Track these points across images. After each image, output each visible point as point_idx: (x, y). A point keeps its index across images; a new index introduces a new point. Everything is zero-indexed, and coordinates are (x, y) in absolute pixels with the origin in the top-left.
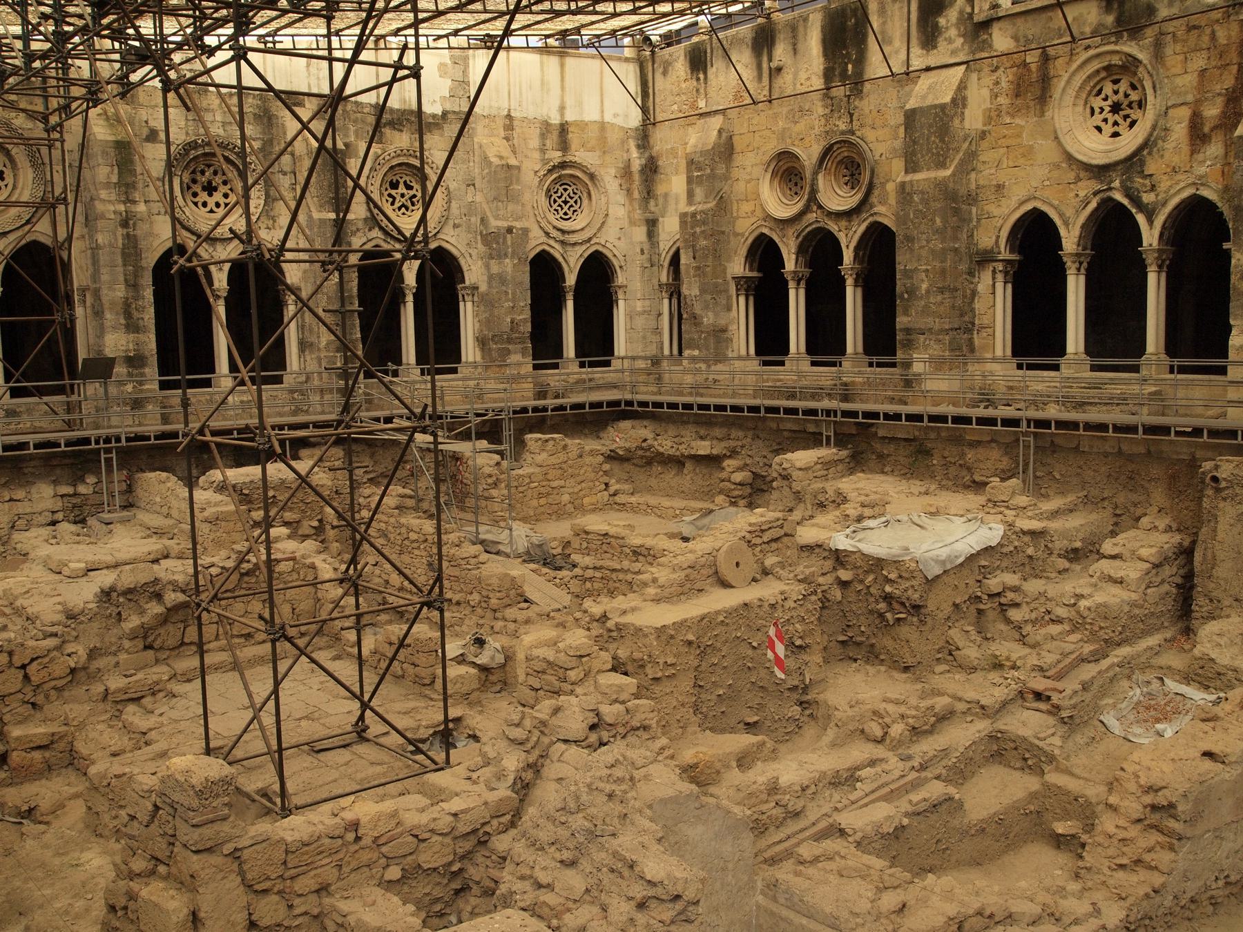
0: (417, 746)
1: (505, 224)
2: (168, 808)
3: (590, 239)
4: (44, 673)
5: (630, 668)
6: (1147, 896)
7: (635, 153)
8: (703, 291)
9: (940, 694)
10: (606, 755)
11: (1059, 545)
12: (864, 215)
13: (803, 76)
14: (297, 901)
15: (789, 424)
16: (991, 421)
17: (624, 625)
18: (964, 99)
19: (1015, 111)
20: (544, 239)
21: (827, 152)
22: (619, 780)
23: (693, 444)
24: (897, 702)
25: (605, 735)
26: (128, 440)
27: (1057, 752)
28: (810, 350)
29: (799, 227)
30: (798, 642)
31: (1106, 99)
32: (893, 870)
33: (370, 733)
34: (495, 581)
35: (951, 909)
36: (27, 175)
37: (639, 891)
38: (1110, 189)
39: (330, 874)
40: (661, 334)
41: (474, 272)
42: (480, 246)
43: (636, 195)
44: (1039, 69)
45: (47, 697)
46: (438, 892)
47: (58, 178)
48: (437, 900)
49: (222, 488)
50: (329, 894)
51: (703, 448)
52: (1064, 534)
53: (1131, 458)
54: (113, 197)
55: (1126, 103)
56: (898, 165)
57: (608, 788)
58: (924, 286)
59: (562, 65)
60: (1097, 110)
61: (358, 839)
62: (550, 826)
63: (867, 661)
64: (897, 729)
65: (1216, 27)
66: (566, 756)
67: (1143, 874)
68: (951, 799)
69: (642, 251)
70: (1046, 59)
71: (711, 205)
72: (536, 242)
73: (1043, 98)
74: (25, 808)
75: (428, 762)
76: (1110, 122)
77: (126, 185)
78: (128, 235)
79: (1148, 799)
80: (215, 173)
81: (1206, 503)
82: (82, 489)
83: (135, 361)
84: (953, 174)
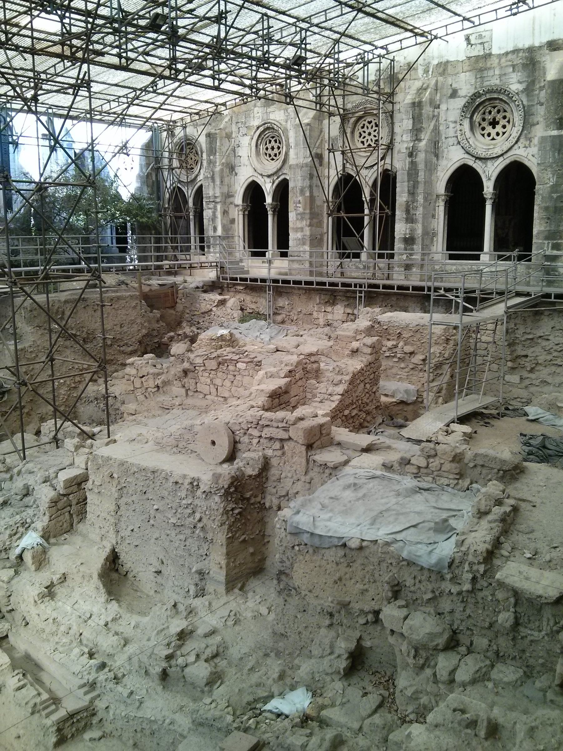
78: (412, 161)
80: (499, 111)
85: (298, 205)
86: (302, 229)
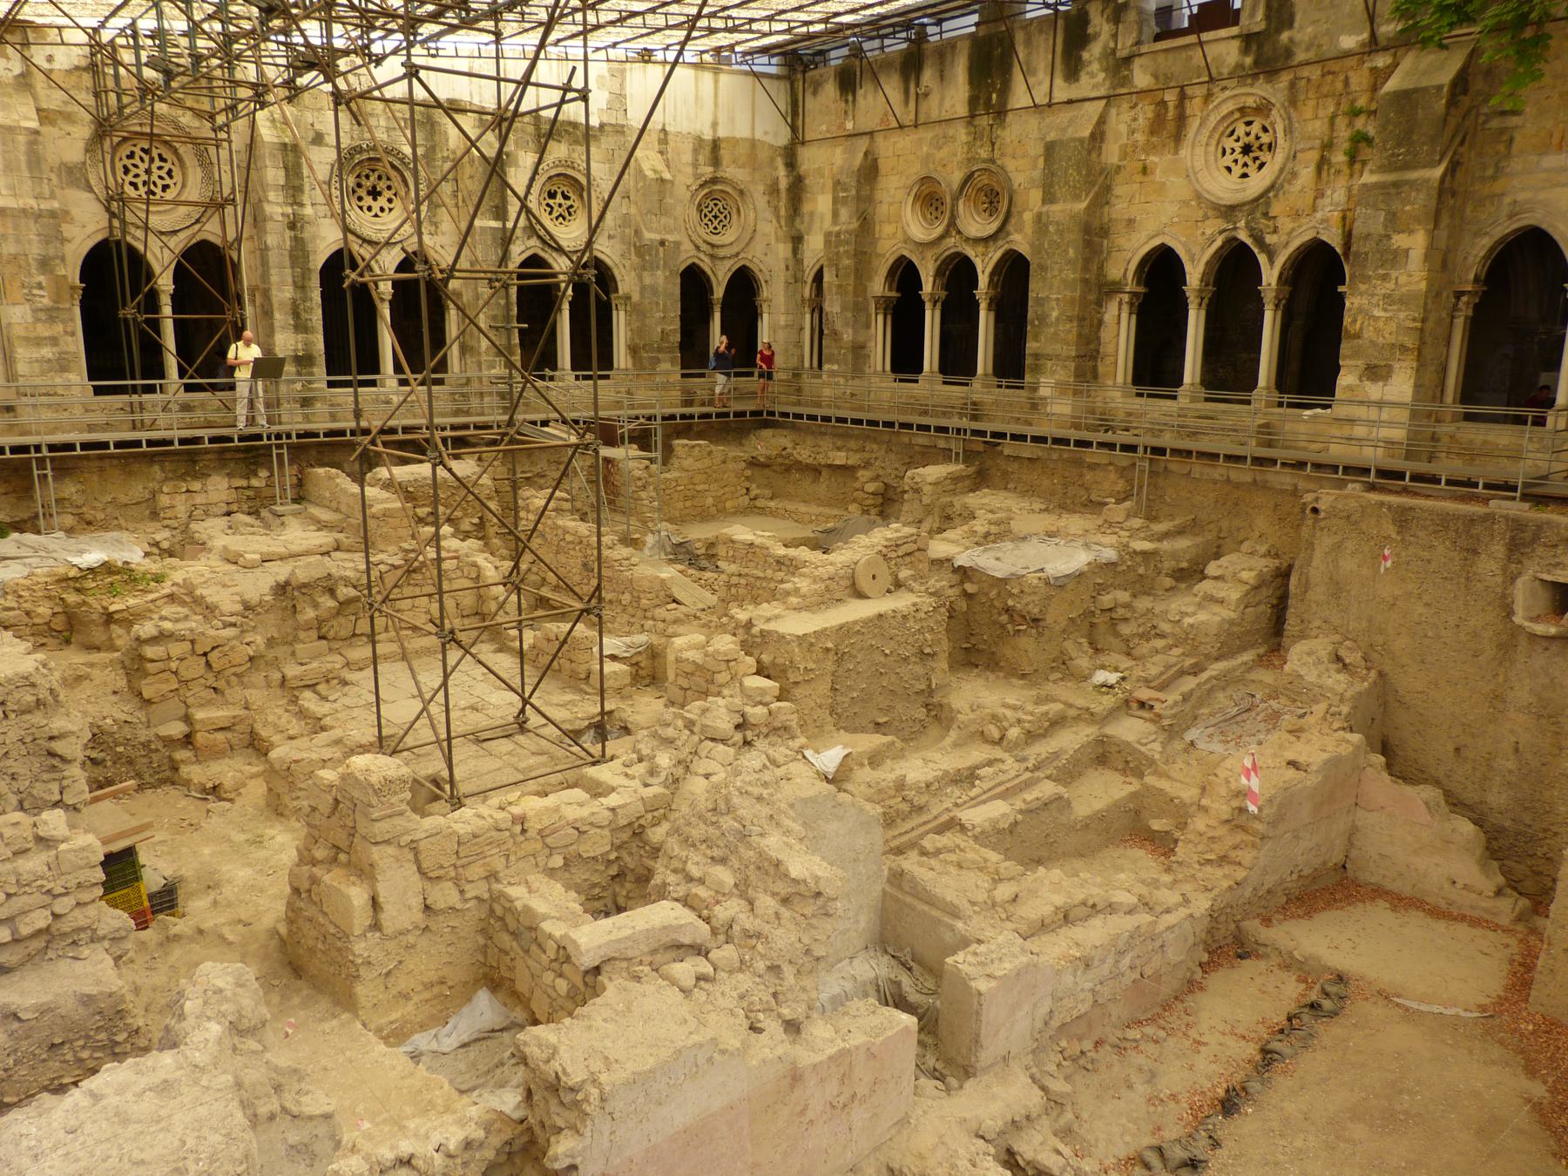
0: (575, 735)
1: (658, 237)
2: (348, 803)
3: (737, 254)
4: (224, 660)
5: (772, 672)
6: (1230, 887)
7: (782, 172)
8: (844, 309)
9: (1055, 701)
10: (753, 760)
11: (1168, 565)
12: (1000, 243)
13: (947, 103)
14: (467, 887)
15: (922, 439)
16: (1112, 446)
17: (769, 632)
18: (1103, 134)
19: (1150, 148)
20: (694, 252)
21: (969, 178)
22: (765, 785)
23: (831, 454)
24: (1015, 708)
25: (749, 735)
26: (299, 436)
27: (1157, 756)
28: (943, 369)
29: (938, 251)
30: (927, 650)
31: (1237, 140)
32: (1008, 863)
33: (529, 725)
34: (646, 584)
35: (1059, 900)
36: (195, 175)
37: (783, 888)
38: (1235, 229)
39: (498, 864)
40: (802, 347)
41: (626, 282)
42: (633, 257)
43: (783, 212)
44: (1176, 107)
45: (228, 683)
46: (596, 879)
47: (226, 178)
48: (594, 886)
49: (388, 485)
50: (498, 880)
51: (840, 458)
52: (1174, 555)
53: (1238, 486)
54: (281, 199)
55: (1256, 145)
56: (1035, 196)
57: (756, 791)
58: (1055, 314)
59: (716, 82)
60: (1228, 151)
61: (524, 831)
62: (702, 826)
63: (988, 667)
64: (1014, 733)
65: (1351, 74)
66: (713, 754)
67: (1227, 869)
68: (1059, 798)
69: (787, 268)
70: (1183, 97)
71: (855, 225)
72: (687, 255)
73: (1178, 137)
74: (210, 785)
75: (583, 754)
76: (1240, 163)
77: (293, 190)
79: (1235, 803)
80: (380, 178)
81: (1305, 532)
82: (255, 482)
83: (304, 361)
84: (1088, 208)
85: (35, 292)
86: (54, 341)
